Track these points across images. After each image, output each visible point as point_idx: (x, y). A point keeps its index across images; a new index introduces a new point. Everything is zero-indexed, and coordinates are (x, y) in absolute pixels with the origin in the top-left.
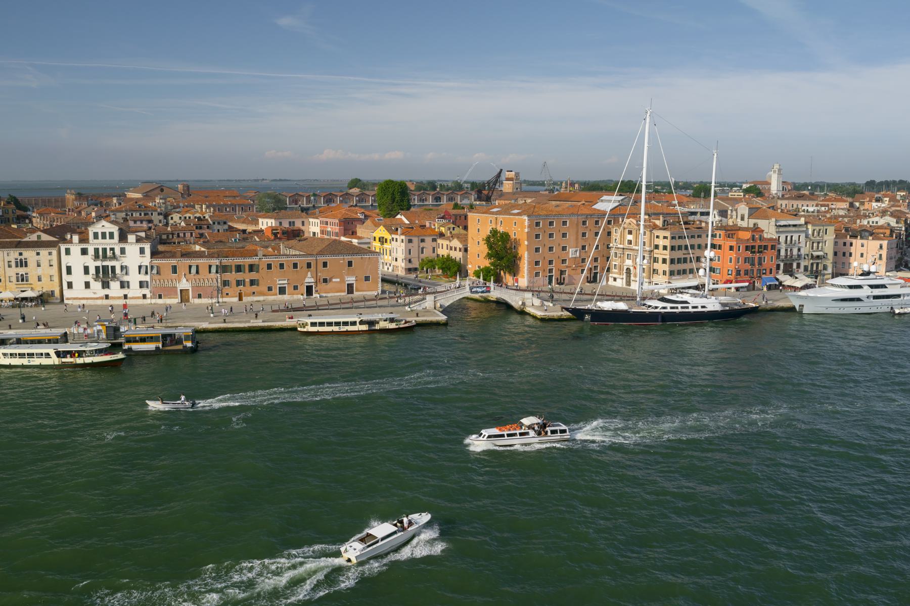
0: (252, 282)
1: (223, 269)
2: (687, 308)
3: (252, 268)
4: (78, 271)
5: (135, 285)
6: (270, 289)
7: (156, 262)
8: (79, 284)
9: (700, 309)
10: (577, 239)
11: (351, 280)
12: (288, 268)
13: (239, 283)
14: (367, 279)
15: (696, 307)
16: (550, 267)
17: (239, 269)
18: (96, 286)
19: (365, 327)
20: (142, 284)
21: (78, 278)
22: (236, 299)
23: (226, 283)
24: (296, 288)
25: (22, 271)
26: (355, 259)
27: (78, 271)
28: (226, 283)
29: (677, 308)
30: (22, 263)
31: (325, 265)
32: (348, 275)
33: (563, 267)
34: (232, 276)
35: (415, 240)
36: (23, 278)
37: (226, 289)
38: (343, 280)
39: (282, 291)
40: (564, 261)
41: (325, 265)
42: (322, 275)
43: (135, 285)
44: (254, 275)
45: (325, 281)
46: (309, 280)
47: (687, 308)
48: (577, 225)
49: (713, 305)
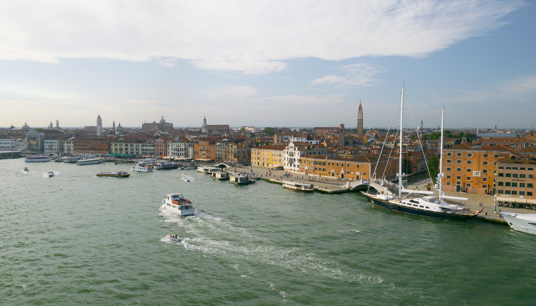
0: (324, 170)
1: (315, 163)
2: (417, 206)
3: (324, 164)
4: (286, 159)
5: (296, 166)
6: (329, 173)
7: (301, 158)
8: (286, 164)
9: (424, 209)
10: (479, 165)
11: (358, 173)
12: (335, 165)
13: (320, 169)
14: (365, 174)
15: (423, 207)
16: (458, 180)
17: (320, 163)
18: (289, 165)
19: (295, 188)
20: (298, 166)
21: (286, 162)
22: (318, 176)
23: (316, 169)
24: (338, 174)
25: (280, 158)
26: (360, 164)
27: (286, 159)
28: (316, 169)
29: (414, 205)
30: (280, 156)
31: (348, 165)
32: (357, 171)
33: (468, 182)
34: (318, 166)
35: (129, 145)
36: (280, 160)
37: (316, 171)
38: (355, 174)
39: (333, 175)
40: (469, 178)
41: (348, 165)
42: (347, 170)
43: (296, 166)
44: (324, 167)
45: (348, 173)
46: (342, 172)
47: (417, 206)
48: (479, 156)
49: (435, 208)
